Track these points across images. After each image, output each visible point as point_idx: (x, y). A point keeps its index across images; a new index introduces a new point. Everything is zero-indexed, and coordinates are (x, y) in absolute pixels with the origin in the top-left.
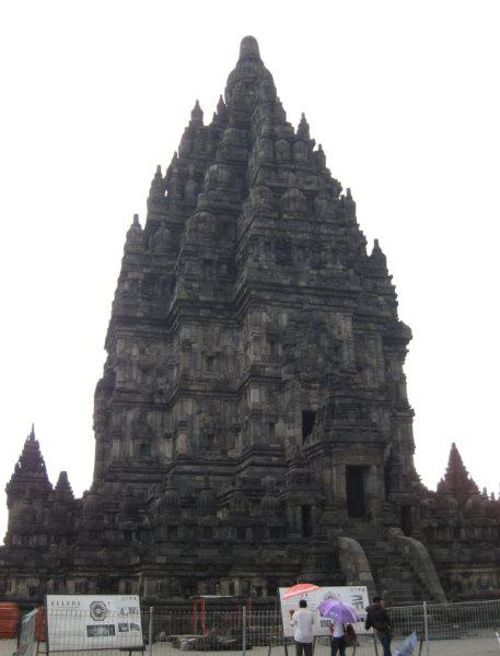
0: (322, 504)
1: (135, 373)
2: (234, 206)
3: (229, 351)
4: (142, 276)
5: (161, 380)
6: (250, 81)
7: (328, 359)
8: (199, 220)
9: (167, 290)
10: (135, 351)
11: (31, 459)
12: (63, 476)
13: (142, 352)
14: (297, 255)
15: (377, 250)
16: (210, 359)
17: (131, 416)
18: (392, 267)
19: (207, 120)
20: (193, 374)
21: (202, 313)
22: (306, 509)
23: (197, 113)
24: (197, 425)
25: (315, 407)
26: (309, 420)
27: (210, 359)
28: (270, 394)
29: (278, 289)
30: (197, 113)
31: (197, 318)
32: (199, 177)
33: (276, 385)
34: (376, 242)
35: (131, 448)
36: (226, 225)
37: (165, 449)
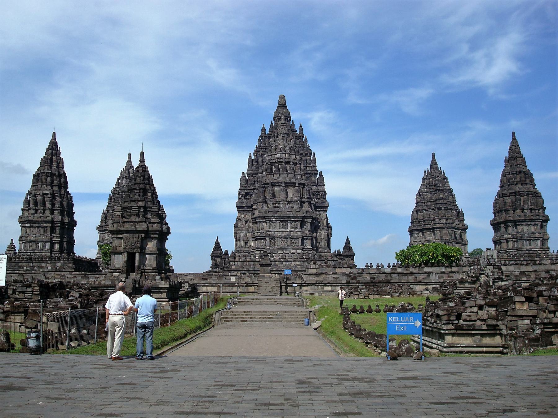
1: (244, 223)
10: (243, 216)
11: (217, 246)
13: (245, 216)
17: (242, 235)
19: (267, 132)
23: (264, 130)
30: (264, 130)
32: (263, 155)
34: (321, 172)
35: (243, 244)
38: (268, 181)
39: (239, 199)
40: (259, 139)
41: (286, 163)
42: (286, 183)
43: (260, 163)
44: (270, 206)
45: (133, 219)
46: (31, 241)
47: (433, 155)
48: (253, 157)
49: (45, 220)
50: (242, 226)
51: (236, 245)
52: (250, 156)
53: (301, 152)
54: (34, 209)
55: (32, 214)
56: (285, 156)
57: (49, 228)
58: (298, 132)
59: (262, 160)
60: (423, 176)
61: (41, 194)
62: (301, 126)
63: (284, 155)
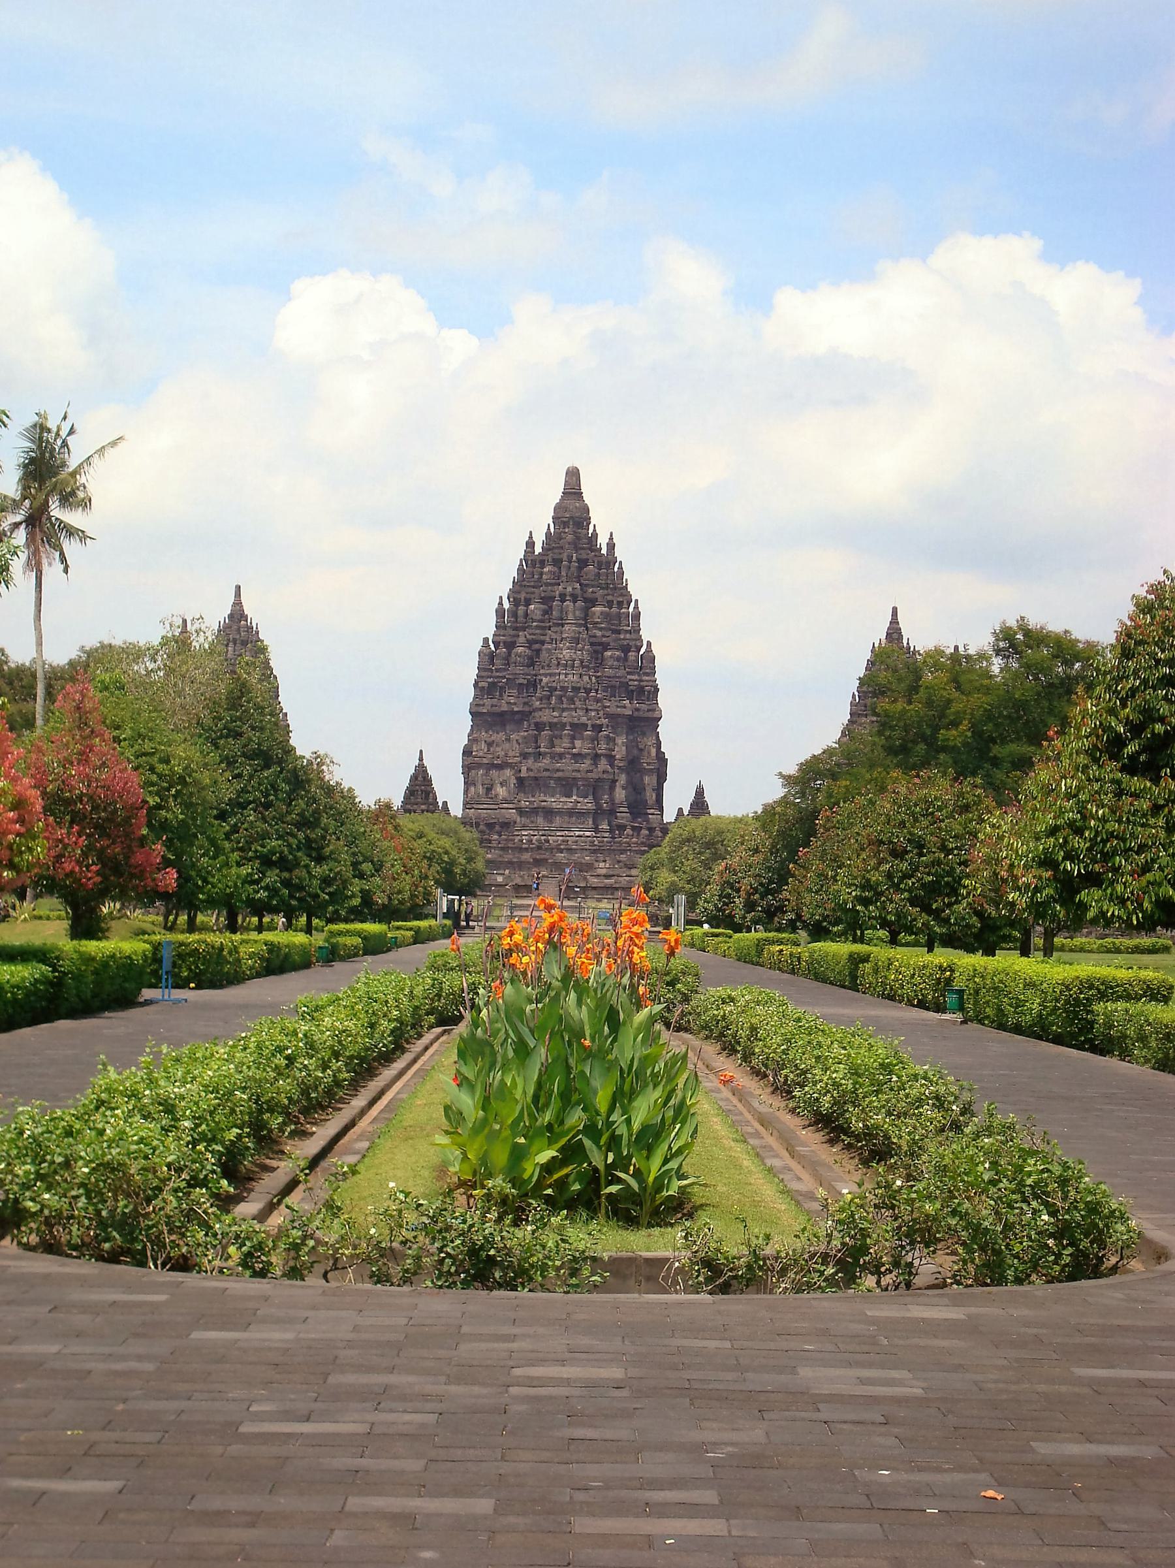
1: (483, 746)
4: (486, 685)
5: (498, 749)
12: (445, 803)
19: (538, 549)
23: (530, 544)
32: (528, 603)
34: (649, 644)
35: (481, 790)
38: (545, 719)
39: (475, 697)
40: (521, 564)
41: (576, 689)
42: (572, 725)
43: (521, 619)
44: (547, 761)
47: (895, 611)
48: (506, 605)
50: (481, 754)
51: (466, 792)
52: (501, 604)
53: (610, 598)
56: (573, 679)
58: (604, 551)
59: (526, 615)
60: (868, 656)
62: (611, 539)
63: (570, 676)
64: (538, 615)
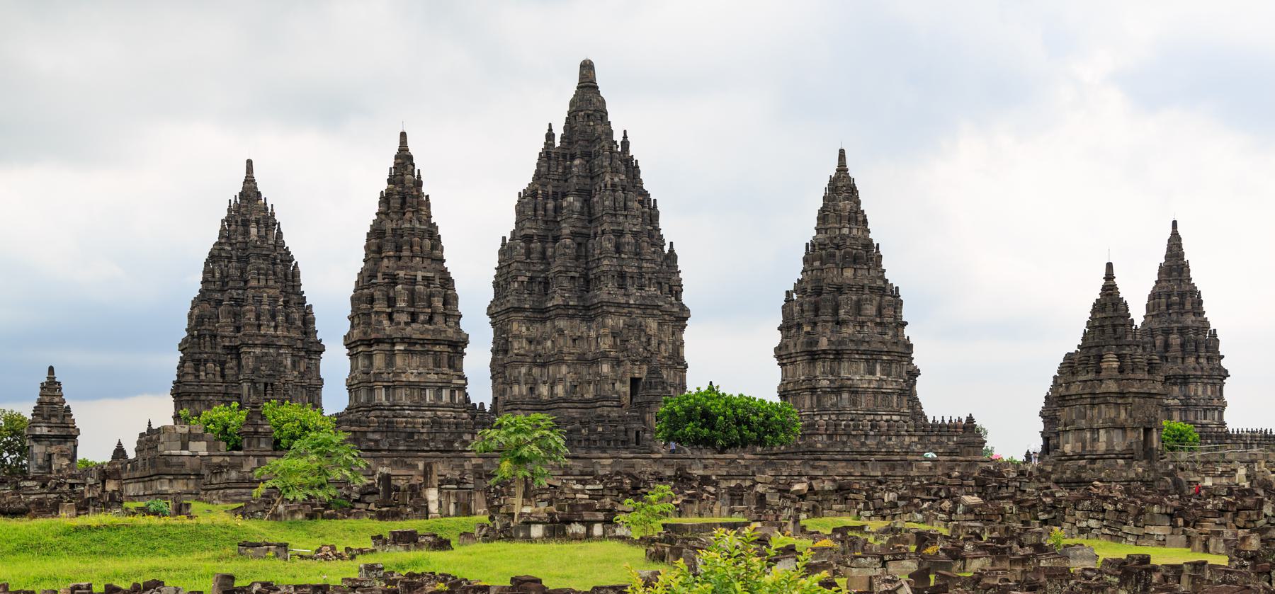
0: (645, 430)
2: (584, 231)
3: (585, 335)
5: (539, 347)
6: (588, 104)
7: (645, 348)
8: (566, 247)
9: (542, 286)
10: (524, 329)
12: (482, 405)
13: (528, 329)
14: (629, 281)
15: (671, 250)
16: (574, 340)
17: (523, 370)
18: (681, 264)
19: (557, 144)
20: (565, 350)
21: (571, 312)
22: (638, 433)
24: (569, 380)
25: (637, 375)
26: (635, 382)
27: (574, 340)
28: (613, 367)
29: (619, 305)
31: (568, 315)
33: (617, 363)
35: (524, 390)
36: (579, 244)
37: (544, 391)
42: (870, 288)
45: (1141, 376)
46: (410, 385)
49: (439, 337)
50: (522, 352)
54: (408, 312)
55: (407, 324)
57: (445, 356)
59: (558, 209)
61: (419, 278)
62: (625, 137)
63: (855, 231)
64: (578, 205)
